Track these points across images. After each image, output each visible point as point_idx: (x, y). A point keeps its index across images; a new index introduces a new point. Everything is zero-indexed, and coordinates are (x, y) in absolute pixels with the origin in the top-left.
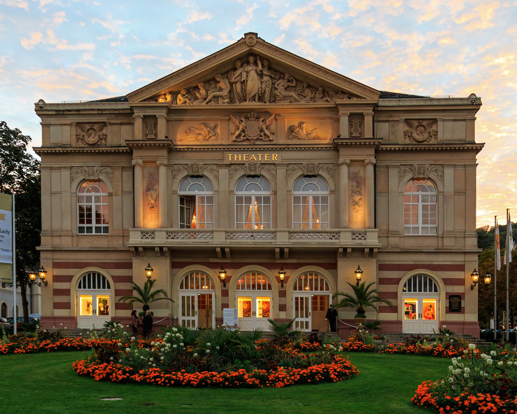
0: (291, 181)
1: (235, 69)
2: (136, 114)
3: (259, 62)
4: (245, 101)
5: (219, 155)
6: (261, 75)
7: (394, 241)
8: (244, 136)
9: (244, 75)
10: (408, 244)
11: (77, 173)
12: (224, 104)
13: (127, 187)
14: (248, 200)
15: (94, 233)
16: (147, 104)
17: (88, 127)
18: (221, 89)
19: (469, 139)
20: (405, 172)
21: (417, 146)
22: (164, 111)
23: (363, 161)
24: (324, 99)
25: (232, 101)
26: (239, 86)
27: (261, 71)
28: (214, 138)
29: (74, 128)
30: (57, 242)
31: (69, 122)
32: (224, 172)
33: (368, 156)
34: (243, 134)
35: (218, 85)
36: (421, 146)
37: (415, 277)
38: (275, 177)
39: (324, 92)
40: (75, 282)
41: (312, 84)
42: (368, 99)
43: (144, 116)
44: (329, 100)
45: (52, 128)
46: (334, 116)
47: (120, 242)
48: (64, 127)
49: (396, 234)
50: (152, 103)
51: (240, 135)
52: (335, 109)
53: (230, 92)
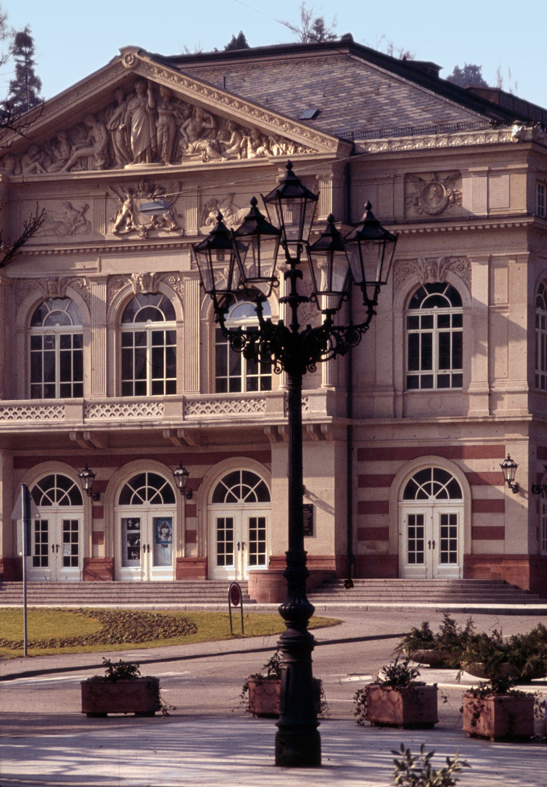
8: (130, 224)
14: (141, 337)
24: (260, 150)
26: (118, 135)
28: (83, 229)
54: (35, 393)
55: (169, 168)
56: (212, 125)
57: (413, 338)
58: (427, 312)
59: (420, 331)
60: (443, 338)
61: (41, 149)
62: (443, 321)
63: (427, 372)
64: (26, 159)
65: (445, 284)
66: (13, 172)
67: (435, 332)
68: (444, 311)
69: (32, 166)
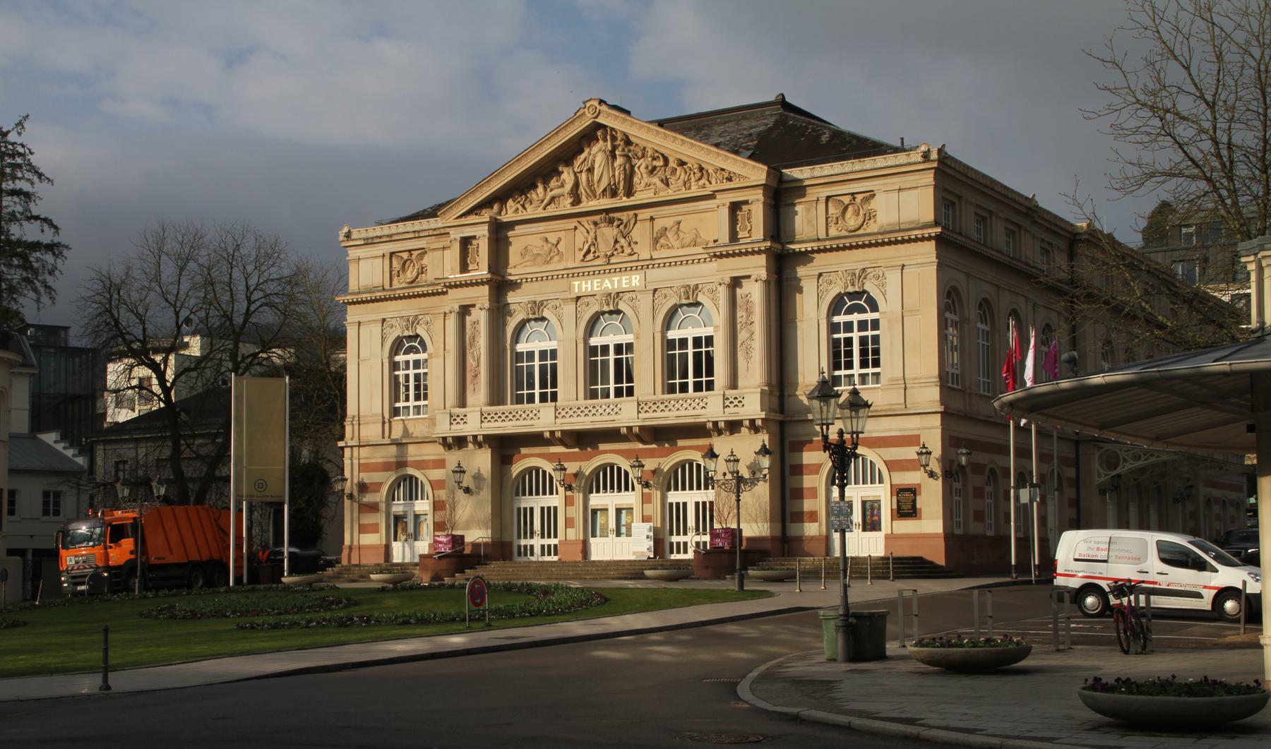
1: (582, 151)
2: (452, 237)
5: (562, 283)
12: (565, 206)
15: (411, 416)
22: (486, 227)
24: (701, 182)
25: (577, 201)
26: (583, 177)
28: (557, 258)
29: (387, 261)
50: (472, 219)
51: (588, 251)
53: (576, 185)
54: (519, 400)
55: (624, 201)
56: (661, 163)
57: (836, 343)
58: (848, 318)
60: (863, 341)
63: (849, 372)
65: (865, 292)
66: (499, 213)
67: (856, 335)
68: (863, 317)
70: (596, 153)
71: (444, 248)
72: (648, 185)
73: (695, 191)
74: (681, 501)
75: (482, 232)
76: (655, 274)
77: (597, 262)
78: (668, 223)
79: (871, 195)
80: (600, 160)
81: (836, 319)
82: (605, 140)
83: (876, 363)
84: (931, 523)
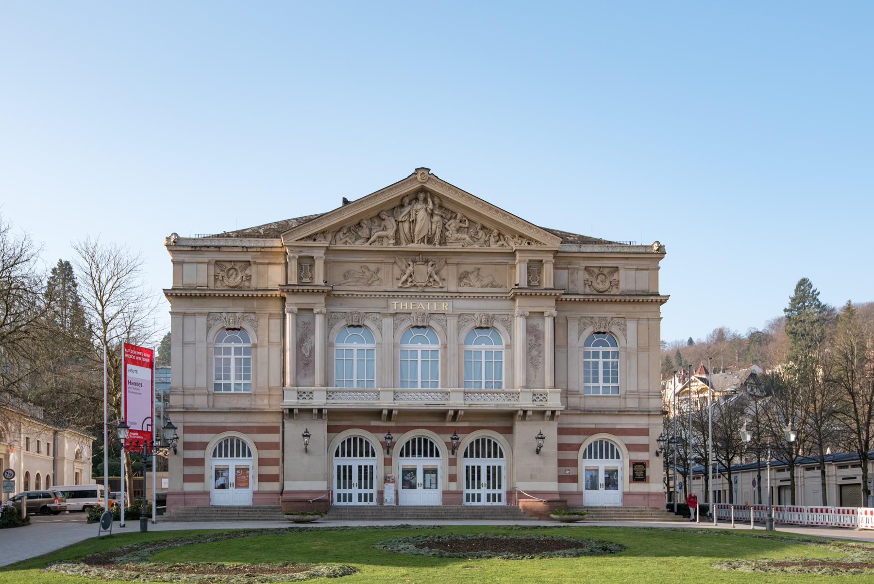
0: (464, 334)
1: (402, 206)
3: (429, 200)
4: (413, 242)
5: (382, 303)
6: (432, 215)
7: (574, 401)
9: (413, 213)
10: (590, 404)
11: (216, 320)
12: (389, 245)
13: (276, 336)
16: (303, 243)
17: (229, 266)
18: (385, 229)
19: (651, 291)
20: (585, 324)
21: (598, 297)
23: (543, 313)
24: (500, 243)
25: (398, 242)
26: (406, 225)
27: (432, 210)
28: (377, 282)
29: (212, 267)
30: (189, 401)
31: (206, 260)
32: (388, 322)
33: (549, 307)
34: (410, 280)
35: (383, 223)
36: (602, 297)
37: (596, 442)
38: (444, 328)
39: (499, 234)
40: (210, 449)
41: (487, 224)
42: (549, 245)
43: (300, 257)
44: (505, 244)
45: (185, 266)
46: (510, 262)
47: (266, 402)
48: (200, 266)
49: (576, 393)
50: (310, 243)
51: (407, 280)
52: (513, 254)
53: (397, 231)
55: (438, 248)
56: (467, 225)
58: (596, 349)
59: (591, 360)
60: (605, 365)
61: (349, 230)
62: (606, 355)
64: (341, 234)
67: (601, 361)
69: (344, 241)
70: (420, 212)
71: (269, 264)
72: (458, 240)
73: (494, 247)
74: (476, 464)
75: (319, 255)
76: (460, 304)
77: (412, 290)
78: (469, 268)
79: (616, 269)
80: (422, 215)
81: (588, 349)
82: (425, 201)
83: (615, 380)
84: (656, 485)
